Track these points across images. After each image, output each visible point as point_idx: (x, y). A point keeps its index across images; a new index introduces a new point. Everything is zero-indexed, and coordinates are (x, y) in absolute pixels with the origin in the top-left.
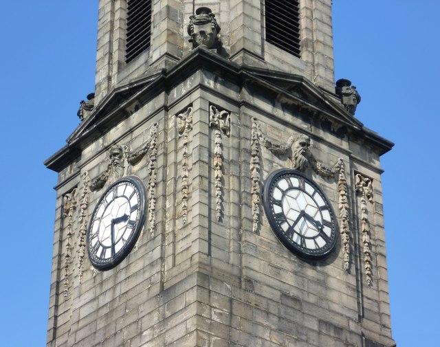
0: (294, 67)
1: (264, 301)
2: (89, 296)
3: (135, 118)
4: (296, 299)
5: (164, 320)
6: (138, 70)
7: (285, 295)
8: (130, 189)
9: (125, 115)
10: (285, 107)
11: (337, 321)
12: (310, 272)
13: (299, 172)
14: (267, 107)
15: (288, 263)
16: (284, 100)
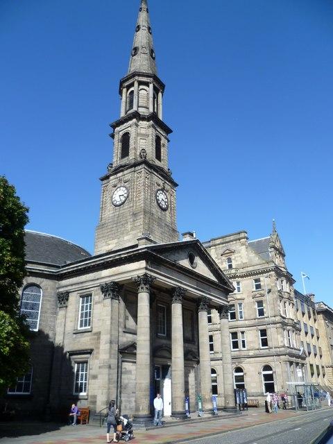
2: (111, 212)
3: (126, 172)
5: (134, 221)
6: (125, 161)
8: (124, 189)
9: (122, 171)
15: (159, 210)
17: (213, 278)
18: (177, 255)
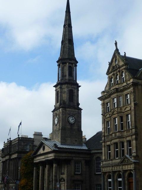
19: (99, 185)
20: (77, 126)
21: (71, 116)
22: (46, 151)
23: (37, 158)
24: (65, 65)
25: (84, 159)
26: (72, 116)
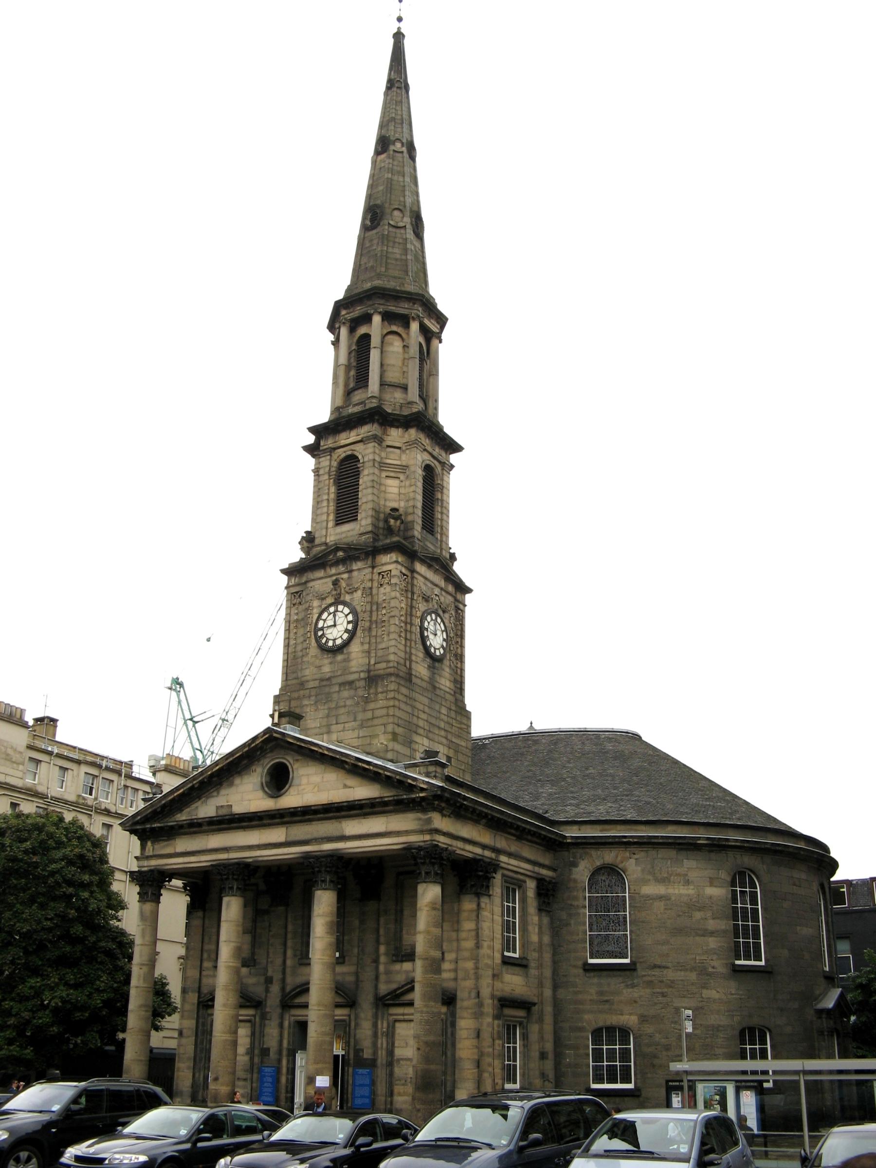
0: (349, 531)
1: (308, 691)
4: (329, 679)
7: (322, 680)
10: (331, 566)
11: (352, 677)
12: (340, 657)
13: (337, 602)
14: (320, 573)
16: (330, 563)
17: (363, 791)
18: (223, 792)
19: (611, 1030)
20: (452, 679)
21: (433, 612)
22: (291, 800)
23: (182, 844)
24: (394, 328)
25: (537, 869)
26: (437, 615)
